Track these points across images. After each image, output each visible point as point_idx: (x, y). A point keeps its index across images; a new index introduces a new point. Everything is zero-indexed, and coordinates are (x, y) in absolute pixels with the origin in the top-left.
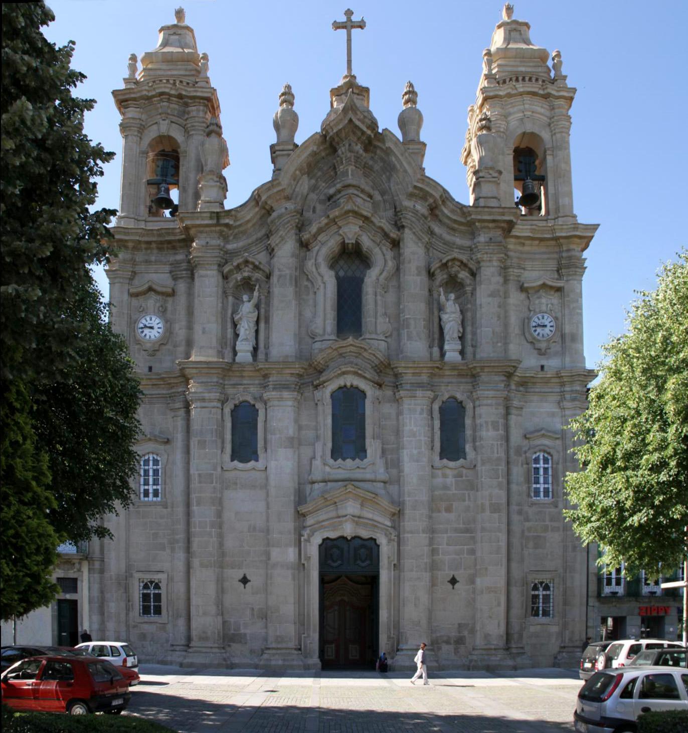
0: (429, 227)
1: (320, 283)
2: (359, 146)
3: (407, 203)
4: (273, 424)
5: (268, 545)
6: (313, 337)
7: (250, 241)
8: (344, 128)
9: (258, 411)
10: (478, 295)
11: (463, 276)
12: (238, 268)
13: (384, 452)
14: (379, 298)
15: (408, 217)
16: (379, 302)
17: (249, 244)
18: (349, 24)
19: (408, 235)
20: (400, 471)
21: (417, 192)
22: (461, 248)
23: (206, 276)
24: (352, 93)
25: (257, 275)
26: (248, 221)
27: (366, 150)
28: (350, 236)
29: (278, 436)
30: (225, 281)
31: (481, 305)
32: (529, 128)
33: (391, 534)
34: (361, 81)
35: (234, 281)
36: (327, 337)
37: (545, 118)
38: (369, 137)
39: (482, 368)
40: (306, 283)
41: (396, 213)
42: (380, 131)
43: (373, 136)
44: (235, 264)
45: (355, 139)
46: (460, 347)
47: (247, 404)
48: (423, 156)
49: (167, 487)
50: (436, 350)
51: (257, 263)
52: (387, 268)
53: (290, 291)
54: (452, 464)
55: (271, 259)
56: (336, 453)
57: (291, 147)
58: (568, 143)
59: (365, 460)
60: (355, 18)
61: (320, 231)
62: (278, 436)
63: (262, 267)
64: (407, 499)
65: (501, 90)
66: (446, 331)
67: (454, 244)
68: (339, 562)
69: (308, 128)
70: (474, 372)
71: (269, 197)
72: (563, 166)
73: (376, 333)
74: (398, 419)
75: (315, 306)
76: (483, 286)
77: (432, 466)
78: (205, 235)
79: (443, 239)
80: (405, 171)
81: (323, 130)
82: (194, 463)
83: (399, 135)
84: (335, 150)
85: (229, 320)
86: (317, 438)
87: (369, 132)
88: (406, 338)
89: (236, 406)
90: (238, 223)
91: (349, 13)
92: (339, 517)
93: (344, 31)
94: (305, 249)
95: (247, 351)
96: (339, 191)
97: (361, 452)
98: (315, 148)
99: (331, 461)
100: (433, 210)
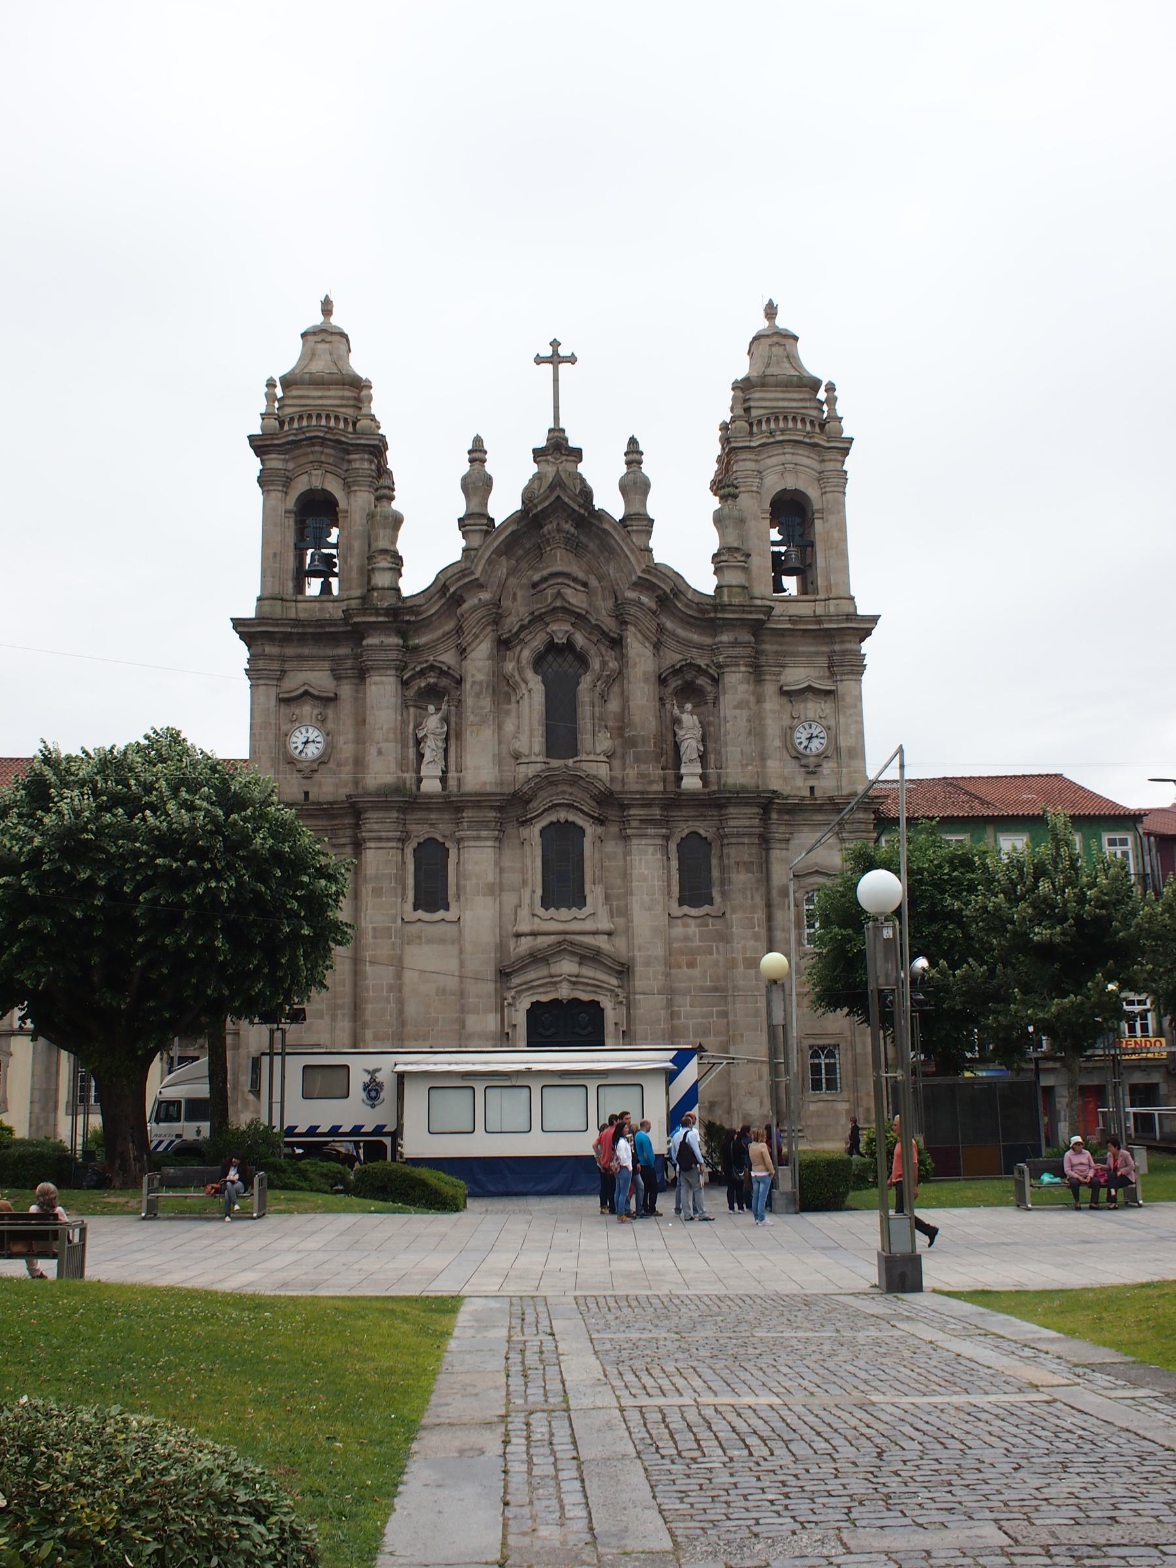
3: (631, 595)
4: (469, 867)
5: (463, 1010)
6: (517, 756)
10: (722, 706)
12: (422, 673)
13: (607, 897)
15: (632, 611)
18: (555, 359)
20: (630, 921)
22: (700, 647)
23: (382, 683)
24: (558, 450)
25: (444, 682)
29: (474, 881)
32: (791, 483)
36: (533, 758)
38: (582, 516)
40: (507, 689)
44: (418, 669)
53: (487, 703)
54: (693, 912)
56: (546, 904)
57: (485, 521)
60: (563, 351)
61: (523, 628)
62: (474, 881)
64: (637, 954)
66: (682, 750)
67: (691, 642)
68: (553, 1030)
72: (836, 534)
74: (625, 860)
79: (678, 637)
87: (582, 511)
89: (419, 844)
91: (555, 344)
92: (552, 976)
93: (549, 367)
95: (435, 777)
96: (545, 579)
99: (541, 911)
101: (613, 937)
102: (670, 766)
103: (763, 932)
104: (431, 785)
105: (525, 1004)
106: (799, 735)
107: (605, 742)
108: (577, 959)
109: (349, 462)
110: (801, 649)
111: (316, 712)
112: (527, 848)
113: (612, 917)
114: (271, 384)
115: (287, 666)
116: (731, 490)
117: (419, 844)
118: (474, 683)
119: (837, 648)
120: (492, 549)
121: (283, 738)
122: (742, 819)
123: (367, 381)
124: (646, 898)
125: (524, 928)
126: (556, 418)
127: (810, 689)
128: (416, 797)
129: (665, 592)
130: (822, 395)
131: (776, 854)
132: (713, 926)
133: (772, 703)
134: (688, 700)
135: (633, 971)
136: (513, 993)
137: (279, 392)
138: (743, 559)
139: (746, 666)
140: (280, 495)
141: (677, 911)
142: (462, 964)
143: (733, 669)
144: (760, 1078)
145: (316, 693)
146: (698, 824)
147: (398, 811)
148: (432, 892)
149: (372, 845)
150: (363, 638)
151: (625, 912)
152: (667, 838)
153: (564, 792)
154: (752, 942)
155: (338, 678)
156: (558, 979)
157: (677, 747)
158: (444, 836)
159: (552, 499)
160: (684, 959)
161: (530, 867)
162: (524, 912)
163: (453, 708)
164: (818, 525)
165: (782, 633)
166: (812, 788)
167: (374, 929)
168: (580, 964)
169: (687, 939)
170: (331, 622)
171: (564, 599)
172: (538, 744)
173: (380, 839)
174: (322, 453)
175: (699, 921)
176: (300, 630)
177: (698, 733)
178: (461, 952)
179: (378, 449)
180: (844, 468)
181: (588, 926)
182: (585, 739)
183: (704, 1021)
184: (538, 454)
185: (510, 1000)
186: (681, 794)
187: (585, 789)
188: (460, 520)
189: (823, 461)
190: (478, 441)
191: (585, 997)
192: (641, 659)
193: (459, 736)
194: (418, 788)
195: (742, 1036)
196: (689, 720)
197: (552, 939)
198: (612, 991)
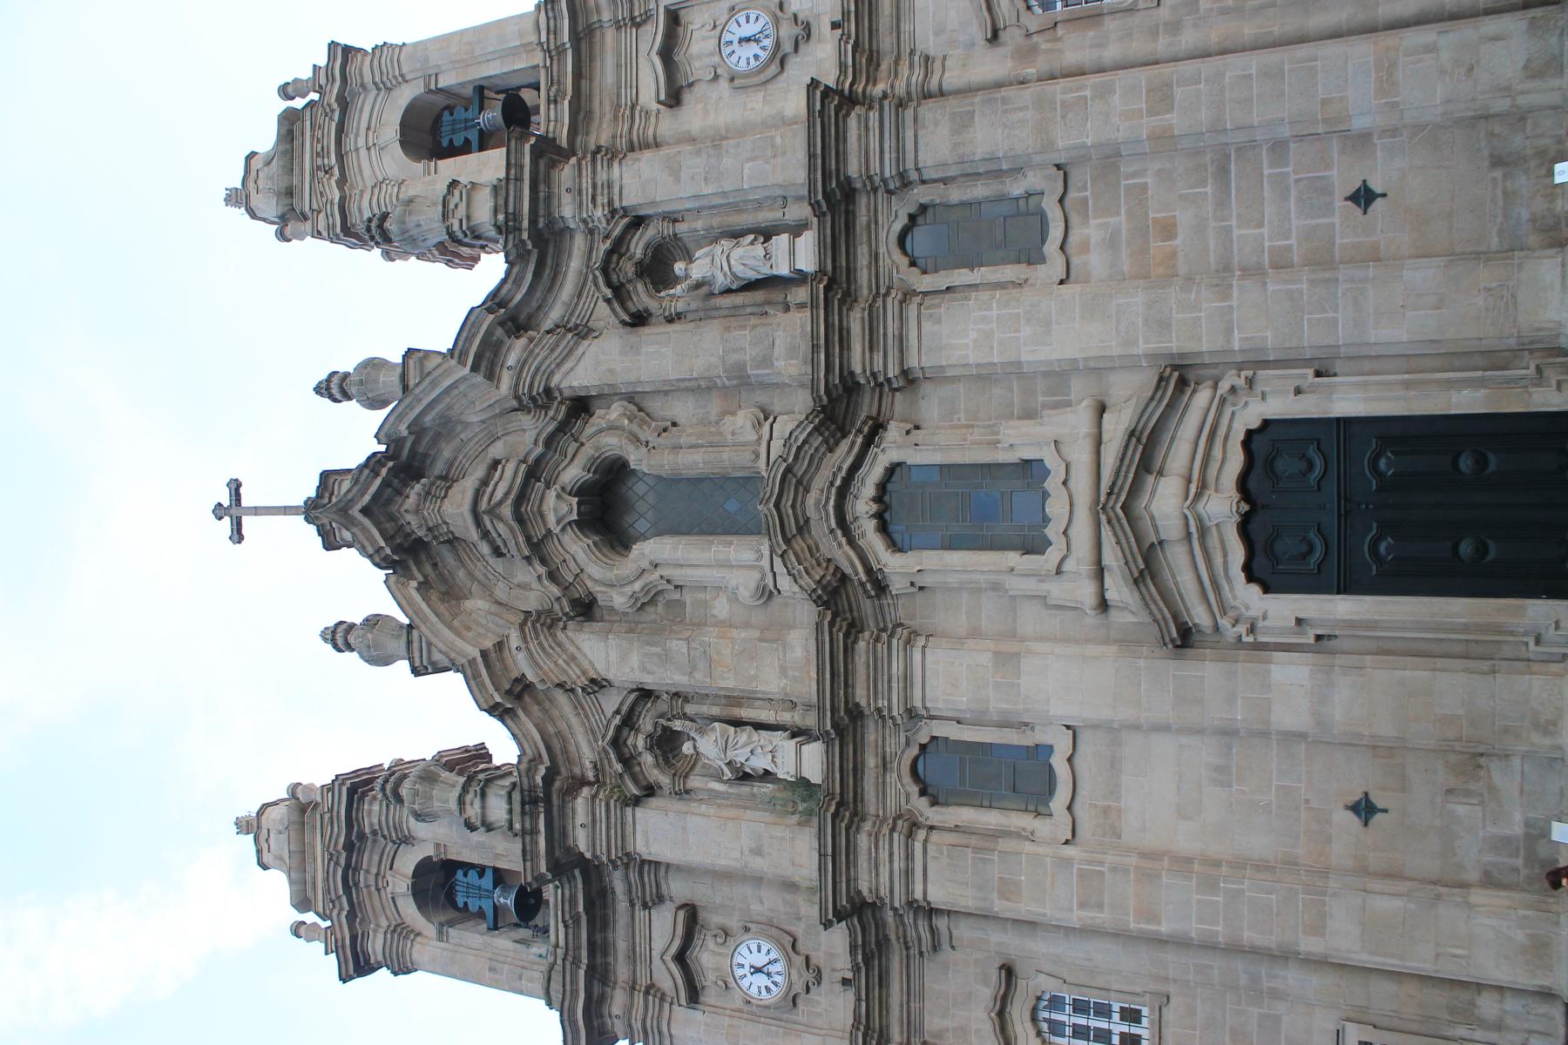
0: (548, 332)
1: (656, 575)
4: (962, 701)
5: (1264, 734)
6: (767, 594)
8: (378, 525)
9: (933, 738)
11: (641, 245)
12: (628, 761)
13: (1029, 415)
16: (693, 440)
25: (646, 723)
27: (418, 476)
28: (564, 508)
33: (1233, 390)
35: (656, 772)
36: (765, 562)
40: (660, 607)
41: (521, 408)
42: (383, 448)
43: (391, 464)
44: (618, 767)
45: (399, 500)
46: (784, 237)
49: (1115, 987)
51: (617, 720)
54: (1056, 232)
58: (416, 45)
59: (1048, 464)
60: (226, 503)
61: (553, 576)
63: (625, 709)
64: (1141, 348)
66: (753, 276)
74: (955, 379)
77: (1062, 282)
82: (1046, 910)
86: (996, 587)
87: (384, 471)
89: (923, 793)
92: (1189, 535)
93: (245, 519)
95: (799, 753)
96: (485, 535)
98: (414, 584)
99: (1053, 555)
101: (1109, 402)
102: (780, 298)
104: (812, 761)
105: (1249, 597)
106: (743, 63)
108: (1150, 479)
109: (374, 833)
110: (610, 78)
111: (711, 944)
113: (1068, 404)
114: (297, 930)
115: (643, 981)
117: (923, 793)
118: (643, 669)
119: (606, 16)
120: (440, 626)
121: (751, 1009)
124: (1026, 331)
125: (1086, 593)
130: (299, 103)
131: (953, 77)
132: (1084, 186)
133: (694, 116)
136: (1224, 623)
137: (310, 918)
138: (457, 193)
139: (610, 166)
140: (417, 947)
142: (1163, 728)
143: (616, 190)
145: (677, 943)
146: (883, 235)
148: (1017, 774)
151: (1058, 377)
152: (908, 295)
154: (1116, 99)
155: (660, 899)
156: (1192, 522)
157: (750, 286)
158: (908, 744)
159: (366, 522)
160: (1157, 246)
161: (965, 577)
162: (1057, 590)
163: (690, 709)
164: (444, 82)
166: (835, 26)
167: (1083, 905)
168: (1161, 473)
169: (1112, 243)
171: (501, 503)
173: (908, 874)
175: (1074, 220)
176: (584, 953)
178: (1135, 727)
179: (357, 786)
181: (1081, 456)
182: (731, 460)
183: (1293, 193)
184: (330, 544)
186: (822, 271)
187: (815, 463)
189: (363, 86)
192: (600, 362)
193: (734, 700)
195: (1324, 102)
197: (1106, 532)
198: (1223, 401)
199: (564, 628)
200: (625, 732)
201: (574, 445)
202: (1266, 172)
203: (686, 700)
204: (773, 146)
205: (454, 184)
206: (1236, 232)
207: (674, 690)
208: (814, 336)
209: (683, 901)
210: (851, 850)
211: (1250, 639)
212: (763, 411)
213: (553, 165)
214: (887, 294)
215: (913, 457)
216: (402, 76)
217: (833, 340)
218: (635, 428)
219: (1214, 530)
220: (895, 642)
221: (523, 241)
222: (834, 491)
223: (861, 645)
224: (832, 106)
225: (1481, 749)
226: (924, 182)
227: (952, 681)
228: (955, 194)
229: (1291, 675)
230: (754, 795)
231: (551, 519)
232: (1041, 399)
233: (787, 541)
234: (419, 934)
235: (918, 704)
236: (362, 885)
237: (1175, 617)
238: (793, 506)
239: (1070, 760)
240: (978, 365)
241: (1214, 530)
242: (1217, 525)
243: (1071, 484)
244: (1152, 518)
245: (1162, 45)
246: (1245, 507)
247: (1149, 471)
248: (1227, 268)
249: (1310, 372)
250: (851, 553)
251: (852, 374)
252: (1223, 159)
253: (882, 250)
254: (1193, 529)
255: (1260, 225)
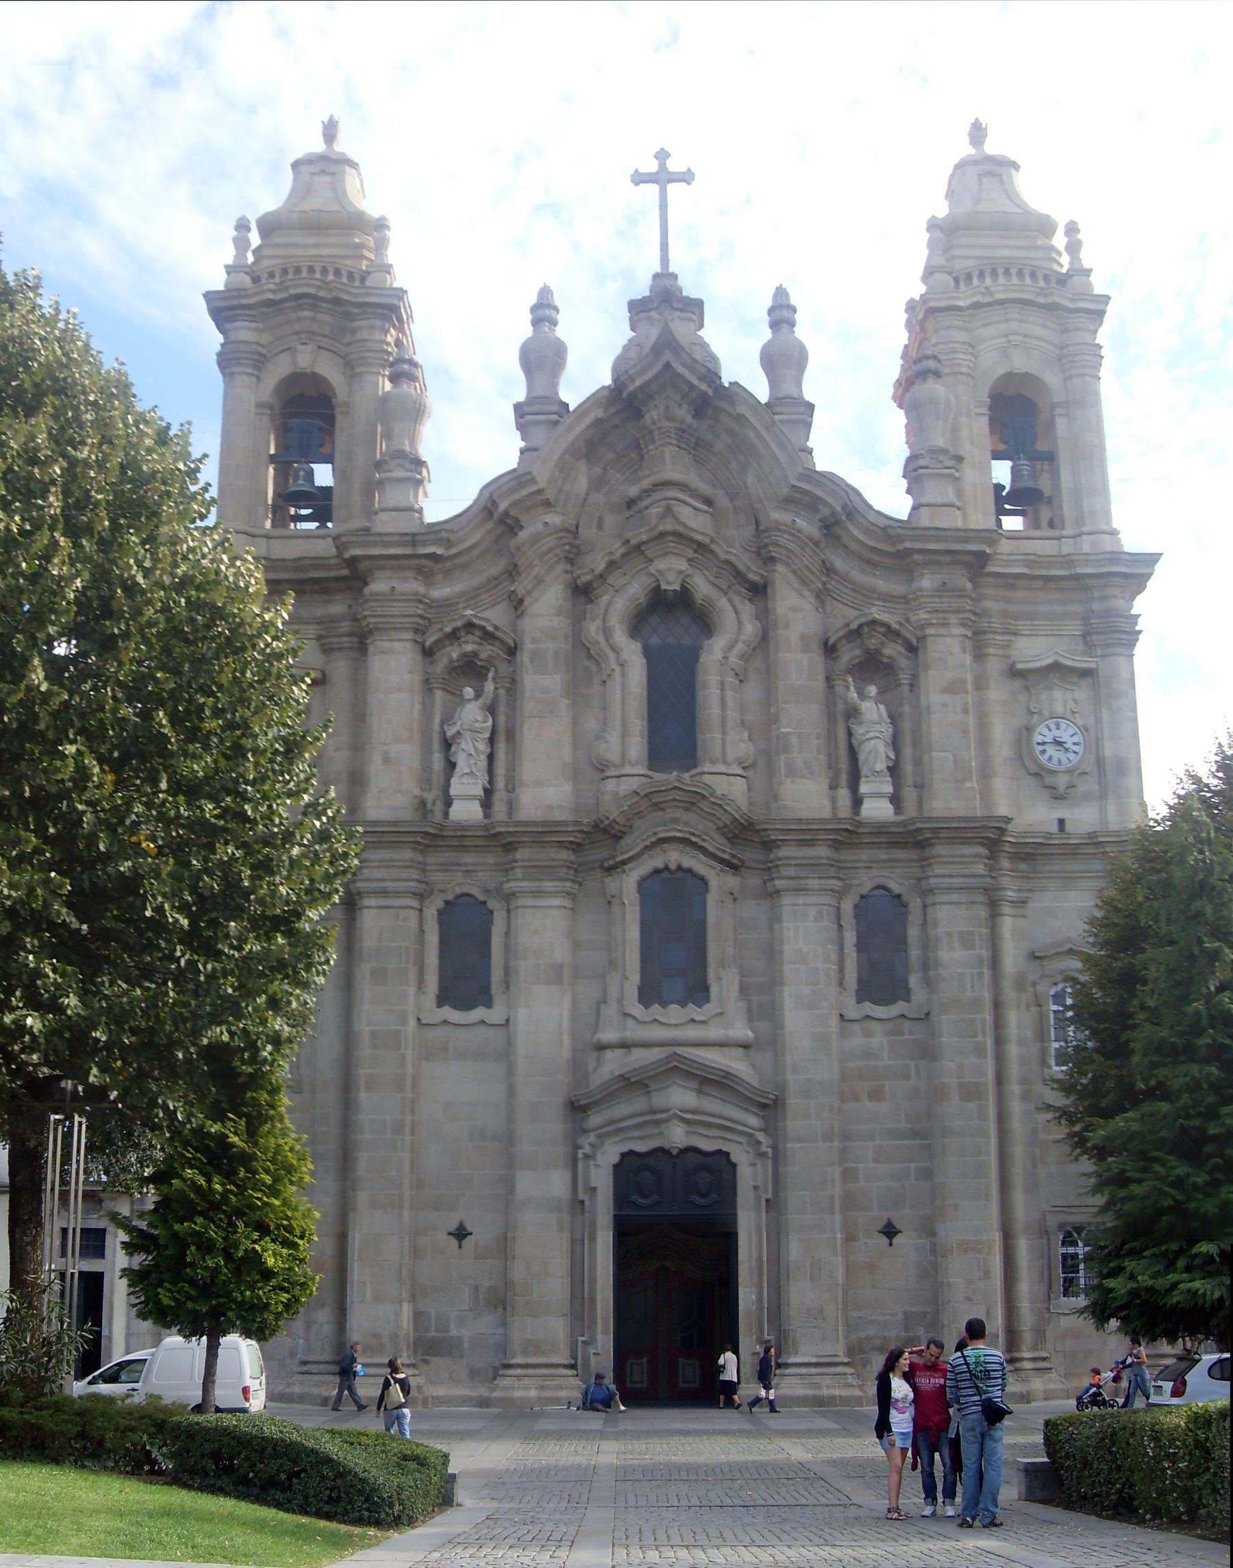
1: (614, 666)
2: (685, 407)
6: (601, 768)
7: (475, 582)
9: (491, 912)
11: (893, 653)
12: (454, 636)
13: (744, 989)
14: (729, 694)
15: (782, 541)
16: (730, 702)
17: (475, 589)
18: (662, 178)
19: (782, 578)
21: (799, 496)
22: (888, 598)
23: (391, 651)
25: (487, 651)
26: (474, 547)
28: (671, 578)
30: (428, 660)
31: (928, 708)
32: (1020, 364)
33: (759, 1143)
34: (690, 290)
35: (445, 661)
36: (627, 770)
37: (1052, 348)
38: (704, 395)
39: (935, 830)
40: (586, 663)
41: (758, 532)
44: (448, 629)
46: (889, 789)
47: (466, 899)
48: (808, 425)
50: (844, 795)
51: (490, 629)
52: (743, 637)
54: (880, 1012)
55: (517, 617)
56: (648, 994)
57: (555, 408)
59: (707, 1006)
61: (612, 565)
65: (959, 298)
66: (862, 757)
67: (874, 591)
68: (655, 1197)
69: (586, 377)
70: (920, 838)
71: (513, 505)
73: (725, 763)
74: (771, 930)
75: (605, 709)
76: (931, 672)
78: (388, 573)
79: (851, 582)
80: (776, 458)
81: (615, 380)
83: (760, 390)
84: (639, 415)
85: (436, 736)
88: (783, 771)
89: (447, 903)
90: (453, 551)
92: (653, 1112)
93: (654, 188)
94: (583, 599)
95: (473, 797)
96: (647, 492)
97: (698, 991)
99: (637, 1010)
100: (830, 528)
101: (751, 1052)
103: (989, 1042)
104: (466, 811)
105: (610, 1154)
107: (740, 746)
108: (695, 1085)
112: (616, 910)
113: (750, 1020)
114: (242, 226)
116: (931, 364)
117: (447, 903)
122: (955, 865)
123: (383, 218)
124: (806, 990)
126: (665, 260)
127: (1056, 667)
128: (442, 827)
129: (833, 514)
134: (870, 681)
135: (784, 1105)
136: (592, 1138)
137: (255, 239)
138: (951, 463)
141: (853, 1010)
142: (511, 1092)
144: (987, 1275)
147: (414, 849)
149: (372, 902)
150: (366, 584)
152: (840, 895)
153: (676, 821)
154: (973, 1059)
155: (327, 650)
156: (664, 1116)
157: (853, 753)
158: (486, 891)
164: (1061, 423)
165: (1010, 582)
167: (373, 1034)
168: (700, 1092)
169: (868, 1054)
170: (317, 562)
172: (637, 747)
173: (384, 893)
174: (313, 319)
175: (888, 1026)
177: (886, 730)
178: (510, 1071)
180: (1097, 342)
182: (711, 739)
184: (638, 309)
185: (587, 1149)
186: (860, 824)
188: (518, 407)
189: (1066, 331)
190: (545, 293)
191: (706, 1145)
192: (797, 612)
193: (511, 735)
194: (446, 815)
195: (956, 1206)
196: (872, 711)
197: (655, 1054)
198: (751, 1135)
199: (566, 572)
200: (477, 633)
201: (725, 587)
202: (912, 1165)
203: (508, 690)
204: (964, 780)
205: (960, 459)
206: (871, 1144)
207: (517, 678)
208: (808, 821)
209: (327, 672)
210: (396, 845)
211: (580, 1155)
212: (751, 766)
213: (968, 565)
214: (839, 879)
215: (712, 899)
216: (1071, 377)
217: (807, 834)
218: (740, 647)
219: (657, 1131)
220: (569, 884)
221: (902, 541)
222: (687, 836)
223: (565, 855)
224: (991, 837)
225: (509, 1309)
226: (925, 907)
227: (540, 929)
228: (913, 933)
229: (558, 1183)
230: (431, 753)
231: (660, 564)
232: (755, 998)
233: (646, 795)
234: (258, 378)
235: (520, 902)
236: (300, 314)
237: (594, 1102)
238: (675, 800)
239: (483, 1022)
240: (782, 951)
241: (657, 1131)
242: (662, 1133)
243: (691, 1025)
244: (667, 1087)
245: (1014, 1088)
246: (675, 1152)
247: (701, 1083)
248: (846, 1136)
249: (770, 1196)
250: (638, 849)
251: (778, 847)
252: (923, 1135)
253: (875, 872)
254: (659, 1116)
255: (875, 1161)
